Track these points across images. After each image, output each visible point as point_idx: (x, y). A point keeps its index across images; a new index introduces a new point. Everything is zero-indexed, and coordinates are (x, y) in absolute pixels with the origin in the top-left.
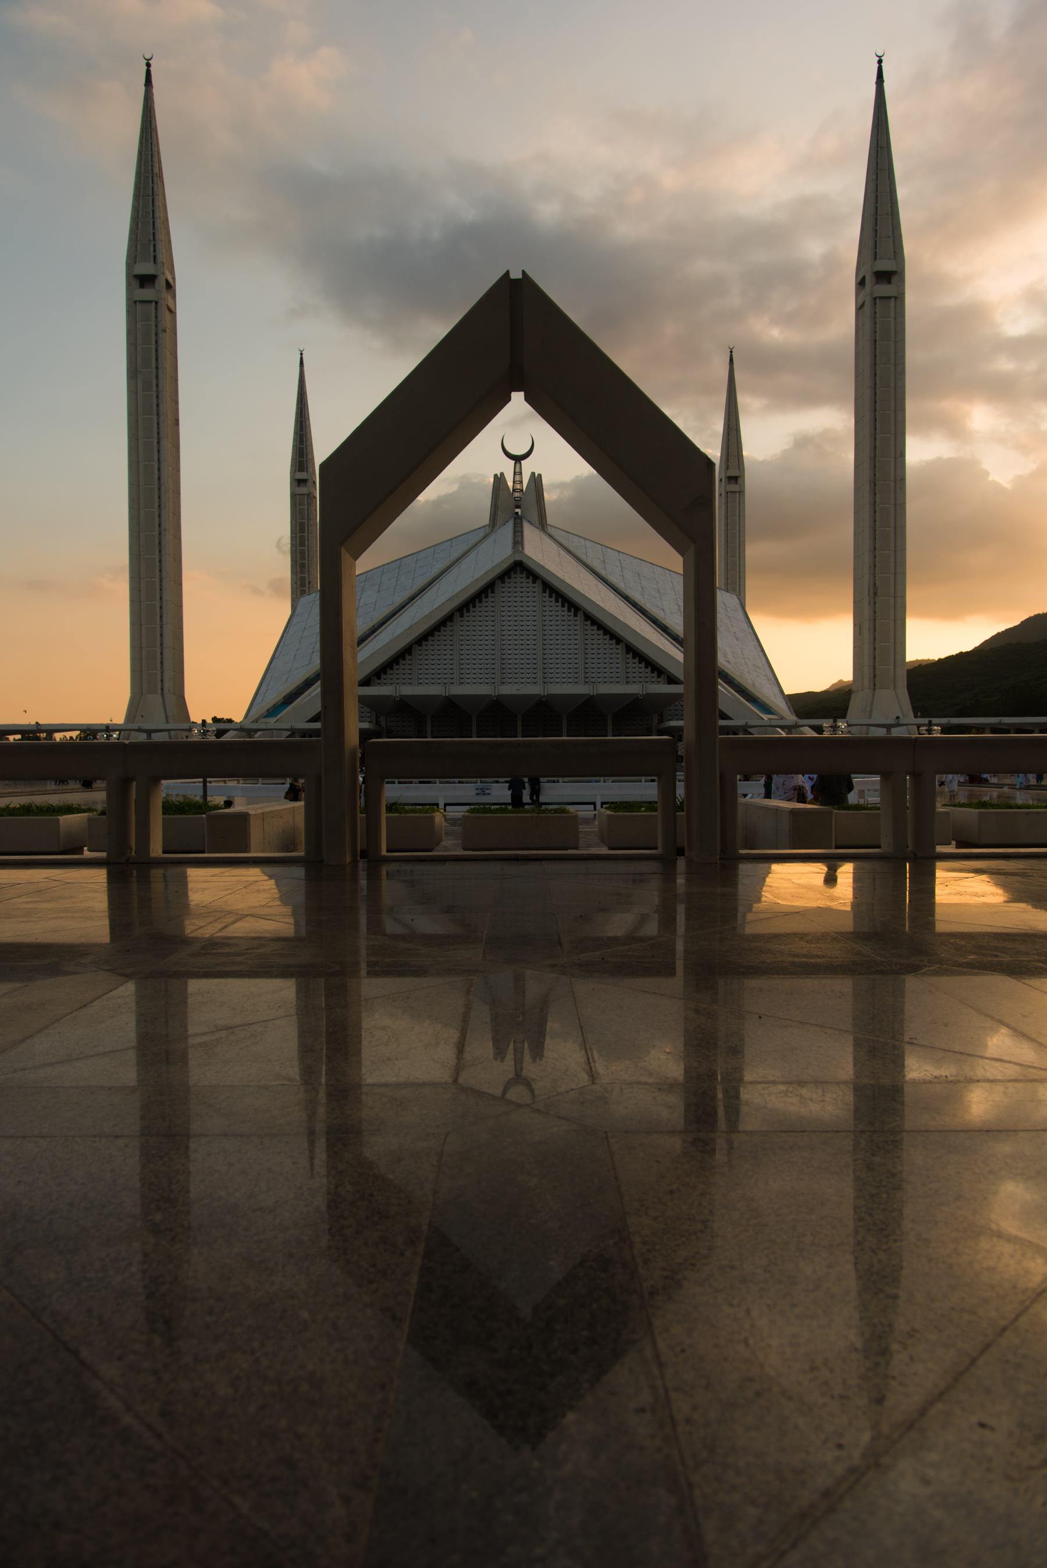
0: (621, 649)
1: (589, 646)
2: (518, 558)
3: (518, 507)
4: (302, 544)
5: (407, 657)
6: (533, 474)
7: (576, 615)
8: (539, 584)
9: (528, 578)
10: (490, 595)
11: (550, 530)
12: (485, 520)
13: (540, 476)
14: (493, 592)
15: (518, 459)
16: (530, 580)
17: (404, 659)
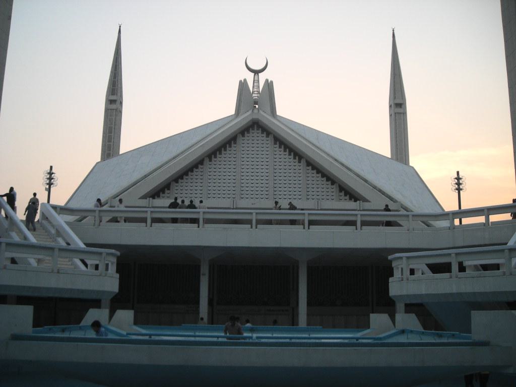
0: (335, 188)
1: (310, 186)
2: (255, 117)
3: (256, 103)
4: (110, 141)
5: (167, 191)
6: (267, 80)
7: (299, 162)
9: (262, 133)
10: (233, 145)
11: (278, 118)
12: (232, 111)
13: (272, 82)
15: (256, 72)
16: (265, 135)
17: (164, 193)
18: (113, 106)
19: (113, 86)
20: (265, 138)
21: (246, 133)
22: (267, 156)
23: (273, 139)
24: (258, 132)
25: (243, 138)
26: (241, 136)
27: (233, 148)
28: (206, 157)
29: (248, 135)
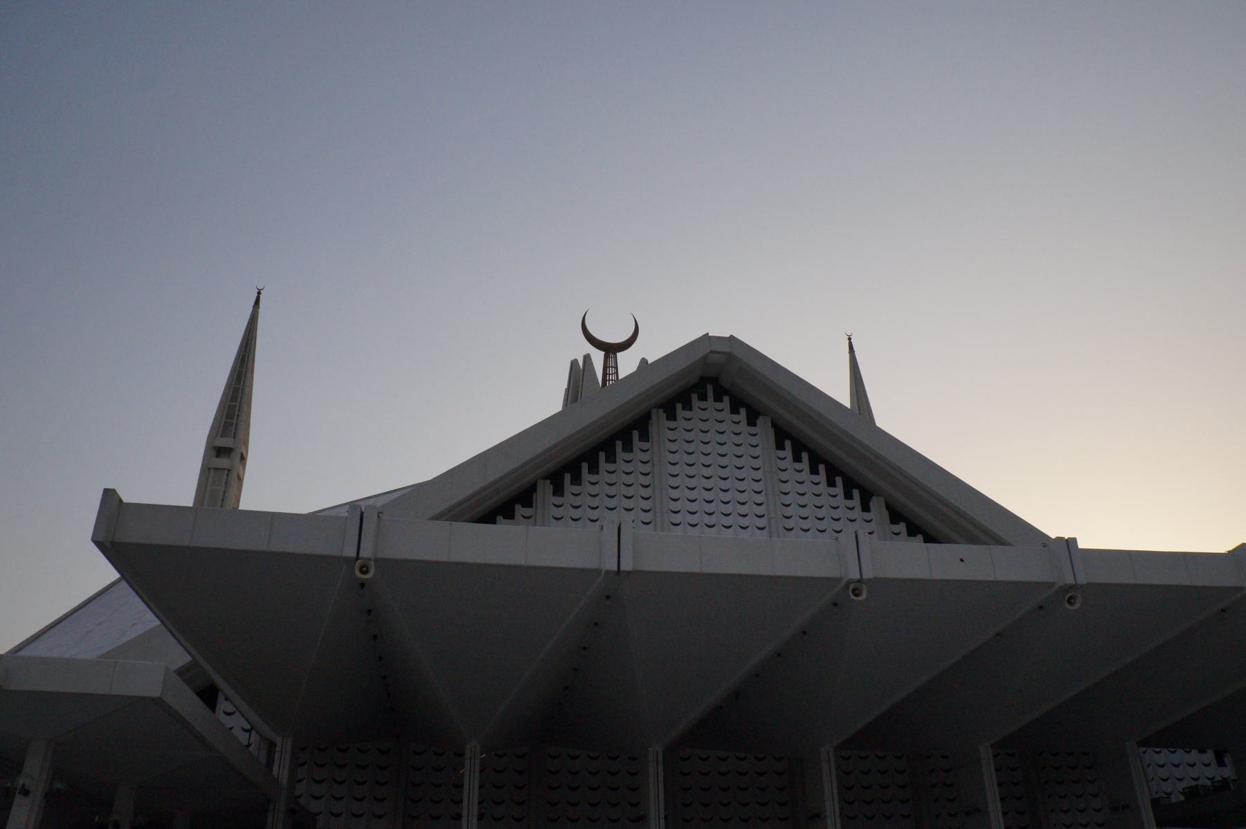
8: (763, 427)
9: (734, 411)
10: (637, 444)
14: (645, 437)
15: (611, 350)
16: (743, 415)
18: (223, 462)
19: (228, 417)
20: (743, 426)
21: (679, 406)
22: (757, 487)
23: (771, 433)
24: (719, 405)
25: (672, 424)
26: (663, 416)
27: (638, 455)
28: (546, 478)
29: (687, 414)
